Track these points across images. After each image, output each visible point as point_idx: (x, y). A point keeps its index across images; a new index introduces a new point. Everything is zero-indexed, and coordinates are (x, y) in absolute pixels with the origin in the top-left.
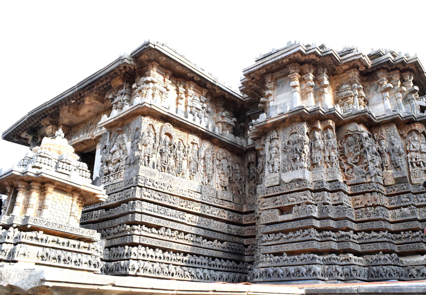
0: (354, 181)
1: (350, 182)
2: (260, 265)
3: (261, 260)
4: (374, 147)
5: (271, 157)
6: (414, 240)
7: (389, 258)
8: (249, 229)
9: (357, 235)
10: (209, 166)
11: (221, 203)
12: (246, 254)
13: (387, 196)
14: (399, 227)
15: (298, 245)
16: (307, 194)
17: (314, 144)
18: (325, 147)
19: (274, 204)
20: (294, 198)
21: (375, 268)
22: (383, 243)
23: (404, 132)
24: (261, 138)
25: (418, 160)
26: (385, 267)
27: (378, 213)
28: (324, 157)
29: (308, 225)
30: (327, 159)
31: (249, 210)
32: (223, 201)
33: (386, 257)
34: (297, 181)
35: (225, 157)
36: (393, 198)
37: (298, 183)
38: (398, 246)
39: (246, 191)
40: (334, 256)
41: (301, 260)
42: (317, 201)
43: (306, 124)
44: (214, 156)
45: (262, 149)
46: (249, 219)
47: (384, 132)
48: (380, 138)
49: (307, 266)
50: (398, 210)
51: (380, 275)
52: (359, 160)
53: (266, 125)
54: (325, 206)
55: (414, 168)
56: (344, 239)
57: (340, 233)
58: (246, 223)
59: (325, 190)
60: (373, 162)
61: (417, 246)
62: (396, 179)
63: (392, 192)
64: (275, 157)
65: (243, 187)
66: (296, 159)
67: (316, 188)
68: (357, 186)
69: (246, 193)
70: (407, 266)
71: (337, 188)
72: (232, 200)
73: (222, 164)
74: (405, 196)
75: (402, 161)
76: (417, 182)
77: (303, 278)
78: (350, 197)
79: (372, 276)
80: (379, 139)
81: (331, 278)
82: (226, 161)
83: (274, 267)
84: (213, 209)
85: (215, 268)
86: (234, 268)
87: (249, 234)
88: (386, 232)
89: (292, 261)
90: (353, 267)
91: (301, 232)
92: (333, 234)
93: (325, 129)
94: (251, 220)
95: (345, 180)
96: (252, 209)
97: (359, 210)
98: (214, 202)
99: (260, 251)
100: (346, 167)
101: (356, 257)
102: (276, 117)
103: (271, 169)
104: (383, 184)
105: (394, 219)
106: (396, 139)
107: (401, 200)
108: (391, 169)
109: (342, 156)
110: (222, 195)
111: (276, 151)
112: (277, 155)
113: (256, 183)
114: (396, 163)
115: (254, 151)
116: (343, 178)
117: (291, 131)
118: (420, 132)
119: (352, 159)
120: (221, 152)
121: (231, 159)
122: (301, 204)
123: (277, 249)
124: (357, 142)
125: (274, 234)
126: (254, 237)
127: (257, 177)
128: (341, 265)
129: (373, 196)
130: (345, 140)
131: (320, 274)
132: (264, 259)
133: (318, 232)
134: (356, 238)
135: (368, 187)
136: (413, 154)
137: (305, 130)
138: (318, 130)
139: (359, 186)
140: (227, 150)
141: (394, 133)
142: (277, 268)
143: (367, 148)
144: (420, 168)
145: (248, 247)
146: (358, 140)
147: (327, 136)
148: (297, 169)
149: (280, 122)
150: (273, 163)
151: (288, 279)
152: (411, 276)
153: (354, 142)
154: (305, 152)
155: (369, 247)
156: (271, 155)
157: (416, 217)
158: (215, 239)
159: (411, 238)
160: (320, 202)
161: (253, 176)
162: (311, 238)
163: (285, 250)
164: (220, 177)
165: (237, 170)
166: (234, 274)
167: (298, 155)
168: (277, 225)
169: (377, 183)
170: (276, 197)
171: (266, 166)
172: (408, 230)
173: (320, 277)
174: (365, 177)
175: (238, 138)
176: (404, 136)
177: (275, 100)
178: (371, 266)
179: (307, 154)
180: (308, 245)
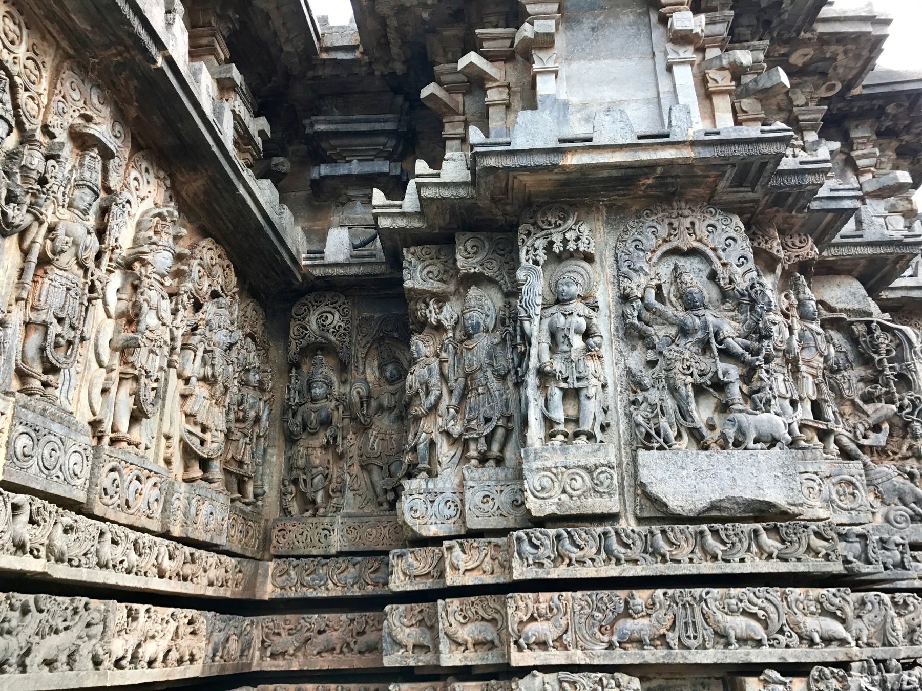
20: (753, 623)
58: (269, 665)
69: (266, 488)
102: (621, 147)
111: (588, 319)
113: (339, 450)
117: (665, 241)
119: (861, 429)
122: (814, 672)
124: (880, 361)
148: (737, 444)
149: (605, 180)
150: (577, 385)
160: (867, 652)
161: (323, 414)
164: (184, 397)
175: (287, 214)
177: (563, 74)
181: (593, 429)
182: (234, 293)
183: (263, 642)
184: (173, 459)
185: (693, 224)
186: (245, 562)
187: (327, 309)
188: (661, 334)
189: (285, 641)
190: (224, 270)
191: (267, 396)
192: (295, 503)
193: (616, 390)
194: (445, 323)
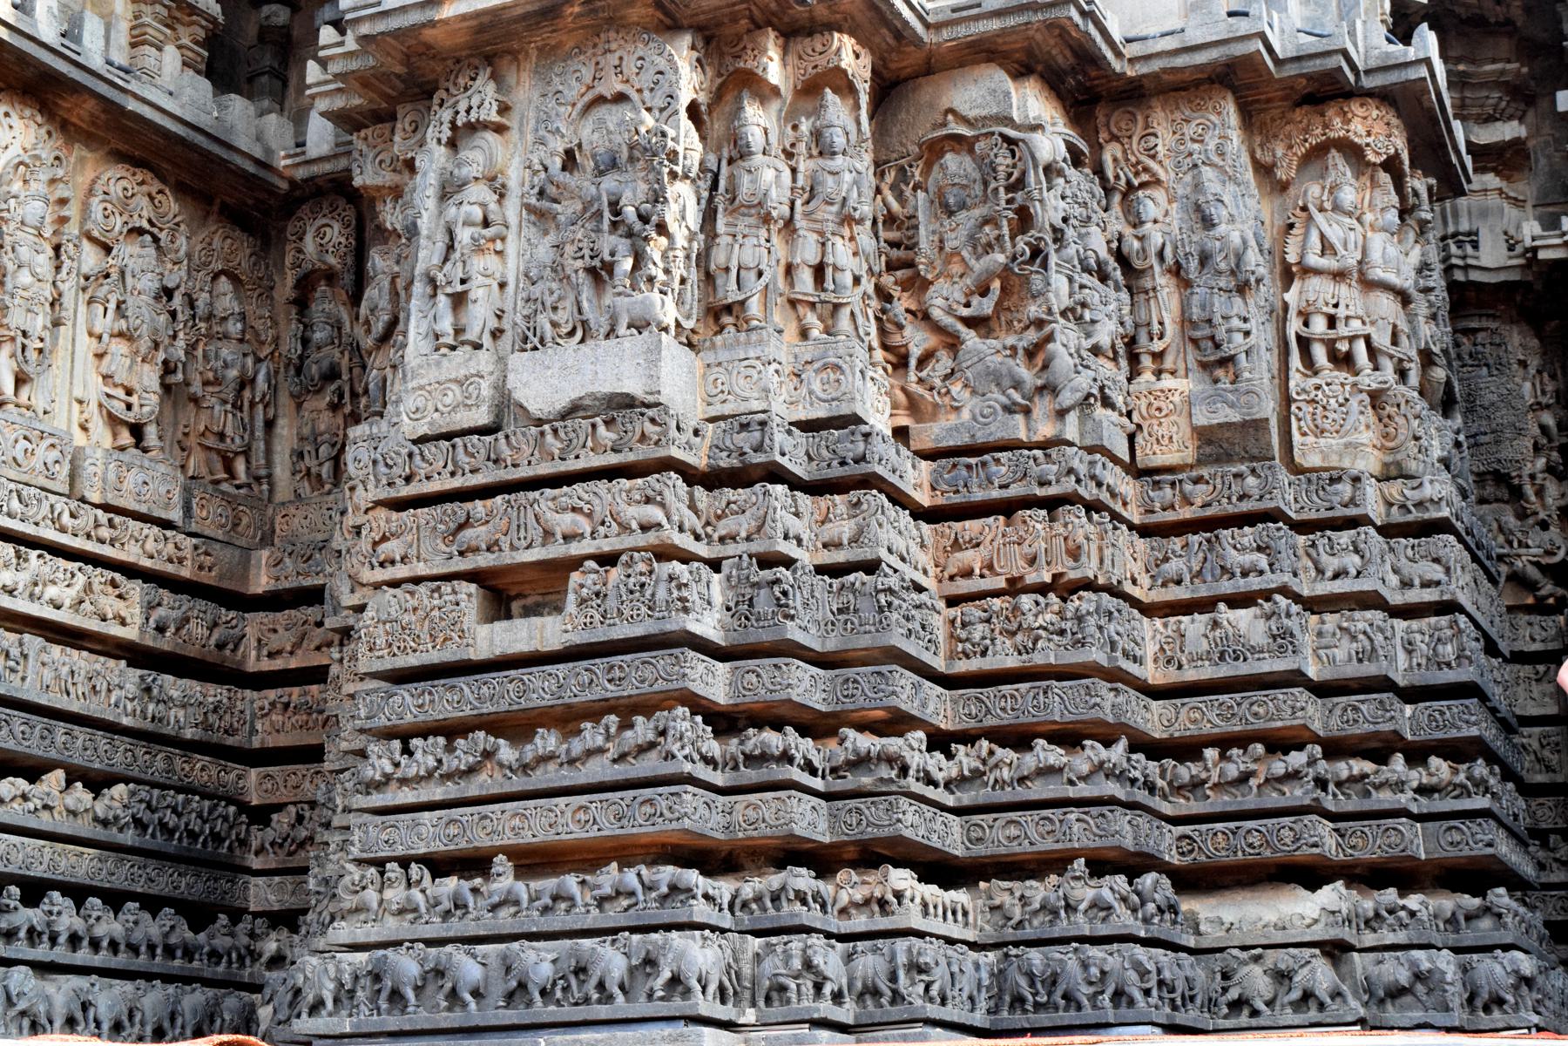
0: (956, 428)
1: (931, 434)
2: (343, 932)
3: (349, 901)
4: (1094, 229)
5: (450, 248)
6: (1273, 799)
7: (1124, 900)
8: (286, 706)
9: (950, 756)
10: (25, 278)
11: (105, 532)
12: (256, 863)
13: (1145, 531)
14: (1194, 722)
15: (585, 808)
16: (667, 493)
17: (732, 177)
18: (798, 203)
19: (454, 549)
20: (580, 518)
21: (1035, 956)
22: (1095, 810)
23: (1279, 153)
24: (392, 117)
25: (1342, 330)
26: (1095, 952)
27: (1082, 629)
28: (789, 270)
29: (656, 687)
30: (805, 279)
31: (287, 585)
32: (118, 519)
33: (1107, 894)
34: (609, 407)
35: (146, 225)
36: (1176, 543)
37: (609, 423)
38: (1181, 830)
39: (277, 458)
40: (802, 879)
41: (602, 901)
42: (722, 540)
43: (693, 48)
44: (65, 212)
45: (397, 193)
46: (284, 639)
47: (1164, 141)
48: (1137, 174)
49: (636, 938)
50: (1201, 620)
51: (1065, 997)
52: (998, 304)
53: (428, 34)
54: (767, 574)
55: (1316, 373)
56: (866, 781)
57: (848, 744)
58: (267, 665)
59: (776, 474)
60: (1079, 319)
61: (1285, 832)
62: (1205, 436)
63: (1172, 507)
64: (479, 250)
65: (259, 433)
66: (609, 268)
67: (724, 462)
68: (973, 461)
70: (1221, 950)
71: (853, 470)
72: (176, 515)
73: (122, 273)
74: (1248, 535)
75: (1252, 325)
76: (1325, 457)
77: (603, 1012)
78: (925, 528)
79: (1018, 1001)
80: (1129, 182)
81: (776, 1012)
82: (151, 251)
83: (430, 943)
84: (47, 569)
85: (42, 952)
86: (169, 951)
87: (283, 741)
88: (1121, 746)
89: (546, 910)
90: (909, 950)
91: (613, 730)
92: (804, 747)
93: (811, 89)
94: (297, 645)
95: (904, 421)
96: (307, 575)
97: (973, 611)
98: (55, 520)
99: (344, 846)
100: (916, 340)
101: (931, 891)
103: (446, 325)
104: (1127, 458)
105: (1172, 669)
106: (1231, 187)
107: (1223, 558)
108: (1182, 372)
109: (899, 273)
110: (112, 476)
111: (483, 205)
112: (489, 232)
114: (1212, 338)
115: (342, 203)
116: (895, 406)
117: (589, 88)
118: (1371, 157)
120: (116, 190)
121: (182, 242)
122: (624, 558)
123: (453, 830)
124: (996, 189)
125: (441, 740)
126: (313, 754)
127: (356, 371)
128: (842, 938)
129: (1058, 527)
130: (927, 171)
131: (712, 988)
132: (371, 896)
133: (717, 734)
134: (940, 777)
135: (1035, 470)
136: (1319, 290)
137: (683, 83)
138: (765, 93)
139: (984, 464)
140: (163, 180)
141: (1222, 155)
142: (449, 948)
143: (1055, 229)
144: (1351, 379)
145: (275, 817)
146: (1002, 175)
147: (817, 135)
150: (459, 288)
151: (516, 1021)
152: (1237, 1005)
153: (978, 189)
154: (673, 227)
155: (1013, 831)
156: (451, 234)
157: (1295, 666)
158: (48, 767)
159: (1259, 786)
160: (742, 547)
161: (325, 364)
162: (668, 769)
163: (506, 842)
164: (100, 356)
165: (224, 319)
166: (171, 989)
167: (623, 245)
168: (460, 682)
169: (1091, 450)
170: (468, 505)
171: (415, 304)
172: (1242, 741)
173: (707, 1006)
174: (1027, 412)
175: (238, 106)
176: (1281, 174)
178: (1016, 944)
179: (681, 241)
180: (648, 809)
181: (480, 338)
182: (177, 224)
183: (259, 641)
184: (88, 425)
185: (621, 58)
186: (218, 546)
187: (325, 221)
188: (570, 211)
189: (284, 639)
190: (152, 198)
191: (266, 351)
192: (306, 484)
193: (517, 286)
194: (398, 227)
